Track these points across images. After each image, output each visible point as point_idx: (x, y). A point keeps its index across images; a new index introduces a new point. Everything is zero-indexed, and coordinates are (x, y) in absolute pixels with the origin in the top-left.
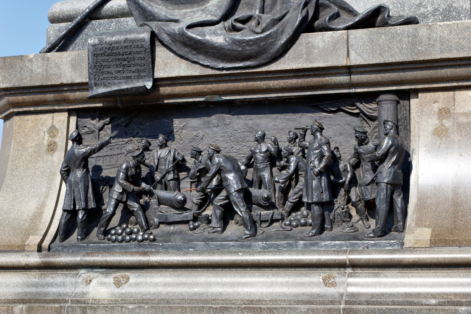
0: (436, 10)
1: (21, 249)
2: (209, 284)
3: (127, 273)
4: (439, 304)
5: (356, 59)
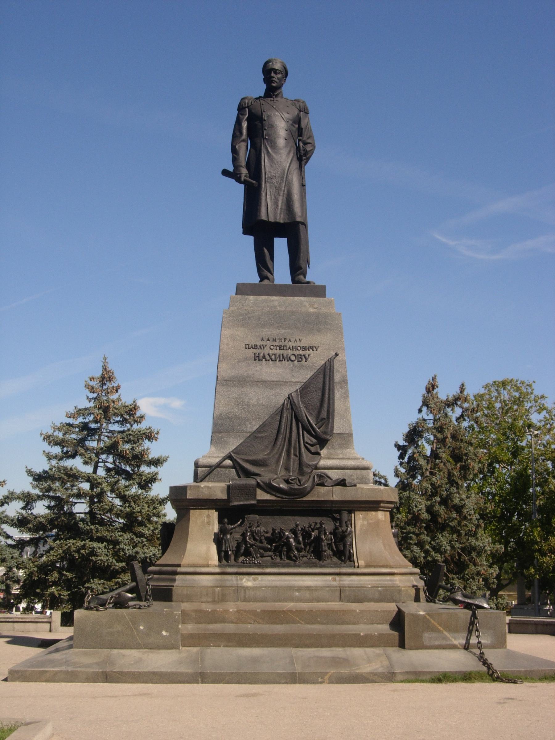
0: (357, 478)
1: (208, 566)
2: (289, 581)
3: (257, 576)
4: (372, 587)
5: (336, 498)
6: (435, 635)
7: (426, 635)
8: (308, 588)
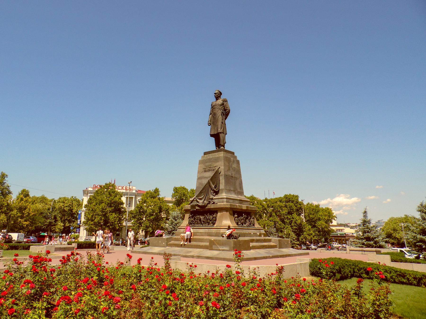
5: (212, 207)
6: (215, 246)
7: (213, 246)
8: (201, 233)
